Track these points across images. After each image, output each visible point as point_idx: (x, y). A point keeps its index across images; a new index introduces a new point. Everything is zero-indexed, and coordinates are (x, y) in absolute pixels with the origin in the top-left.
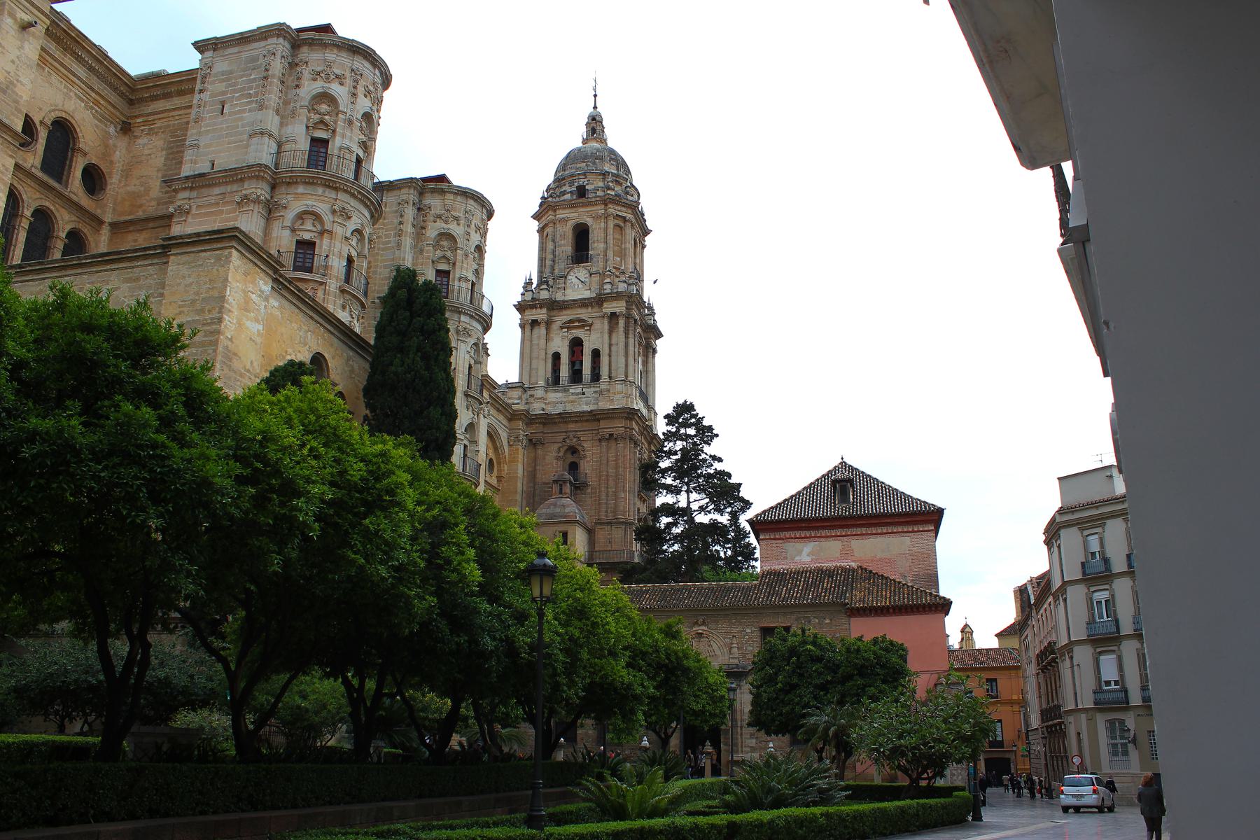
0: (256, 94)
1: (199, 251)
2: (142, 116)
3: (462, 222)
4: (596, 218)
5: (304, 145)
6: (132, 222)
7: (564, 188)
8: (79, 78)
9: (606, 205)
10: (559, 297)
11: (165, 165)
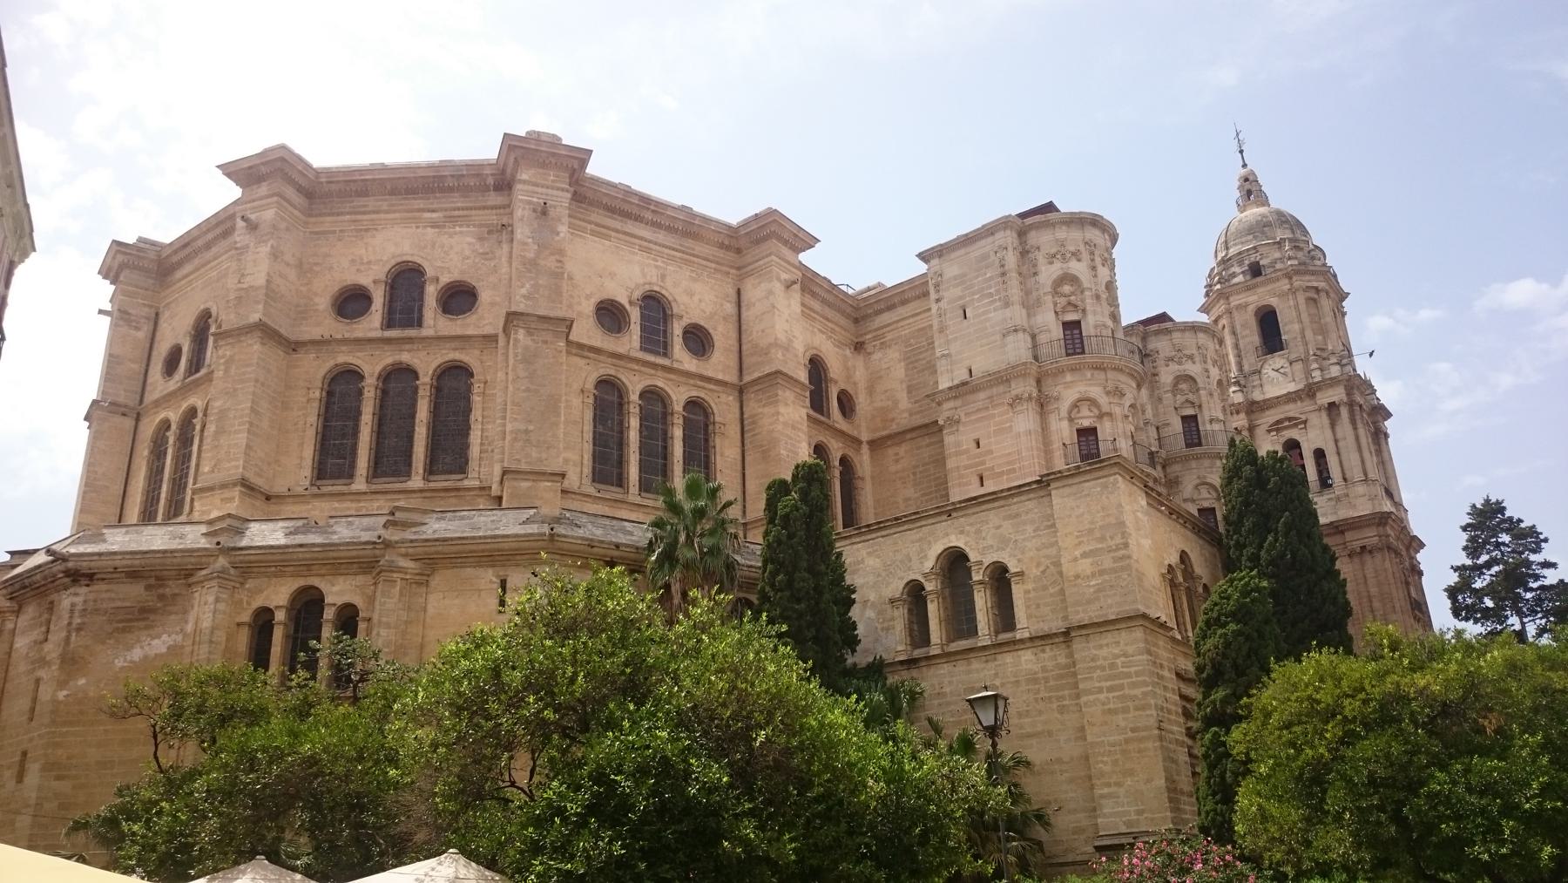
0: (998, 291)
1: (1080, 483)
2: (870, 332)
3: (1197, 359)
4: (1282, 295)
5: (1057, 332)
6: (889, 437)
7: (1233, 269)
8: (817, 313)
9: (1290, 278)
10: (1257, 396)
11: (906, 376)
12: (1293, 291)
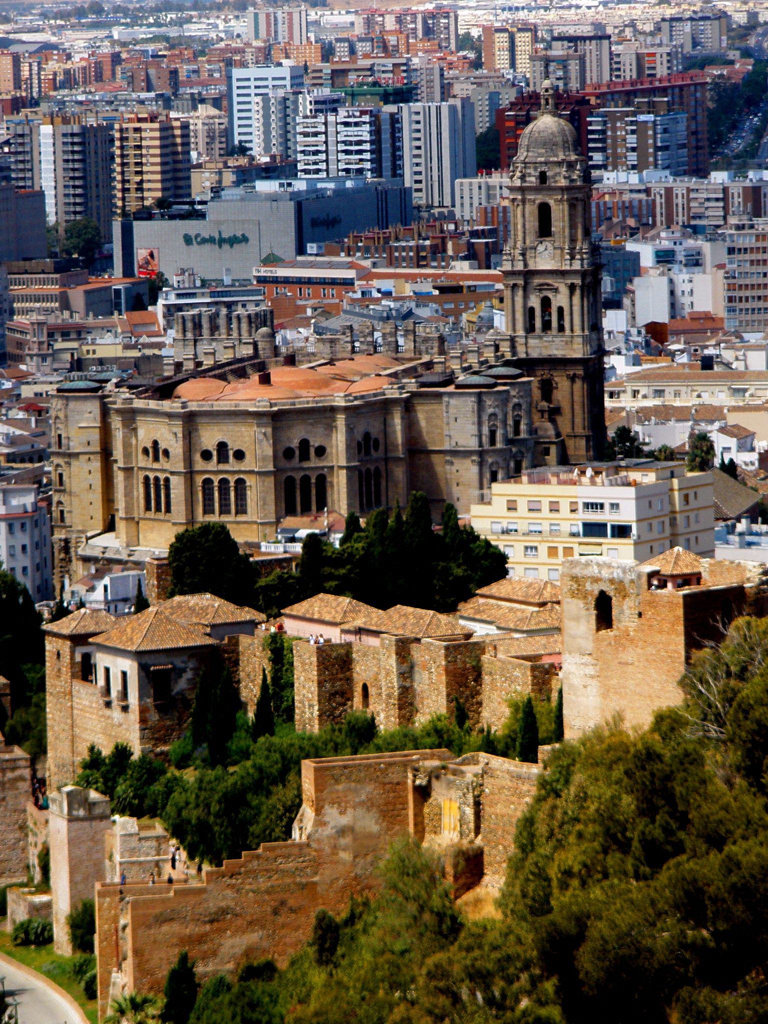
7: (528, 171)
10: (532, 267)
12: (561, 201)
